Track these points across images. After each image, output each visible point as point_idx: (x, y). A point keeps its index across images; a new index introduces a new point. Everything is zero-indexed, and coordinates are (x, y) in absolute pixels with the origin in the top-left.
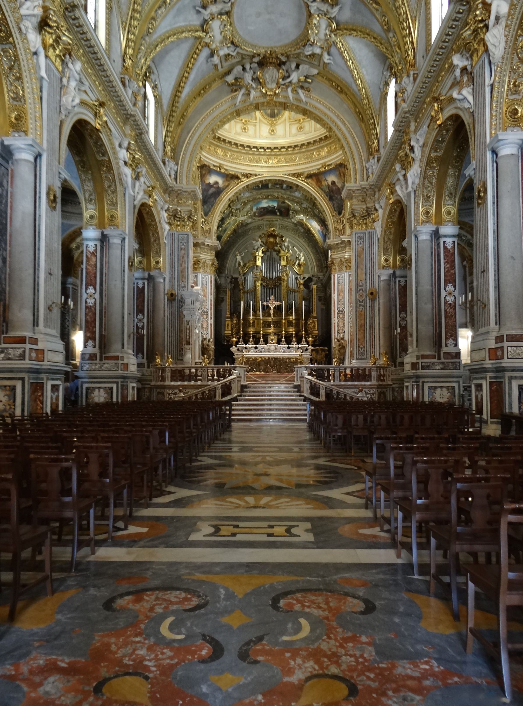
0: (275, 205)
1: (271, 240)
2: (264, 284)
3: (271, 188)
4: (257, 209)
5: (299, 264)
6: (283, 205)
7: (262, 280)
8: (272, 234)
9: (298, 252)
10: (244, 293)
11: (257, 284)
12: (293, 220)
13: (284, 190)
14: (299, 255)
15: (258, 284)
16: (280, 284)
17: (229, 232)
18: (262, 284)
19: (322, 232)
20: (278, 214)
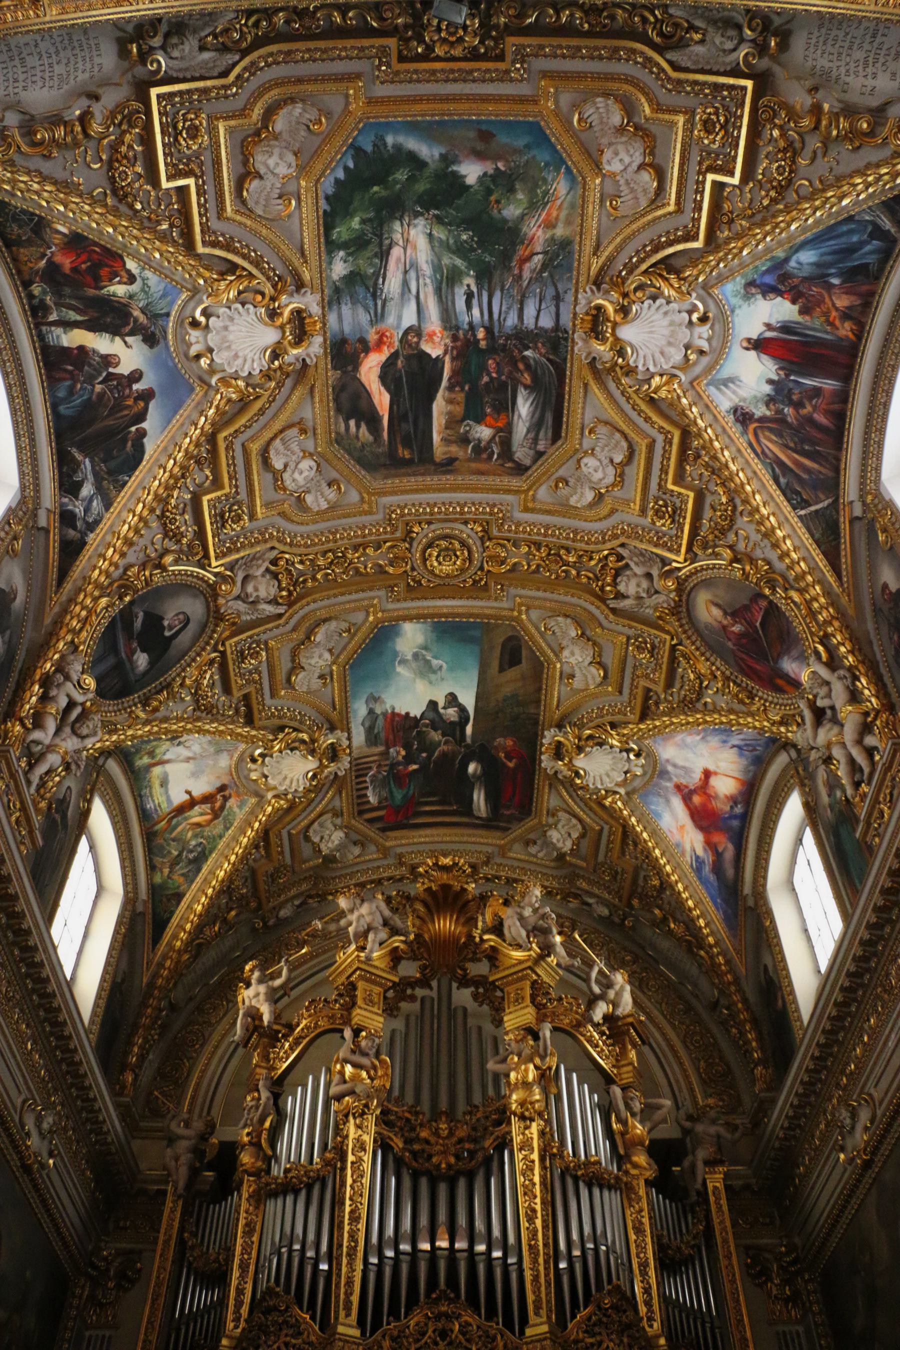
0: (468, 700)
1: (445, 925)
2: (398, 1143)
3: (448, 465)
4: (372, 738)
5: (607, 1018)
6: (510, 682)
7: (385, 1119)
8: (446, 888)
9: (600, 964)
10: (259, 1198)
11: (352, 1131)
12: (554, 835)
13: (520, 470)
14: (607, 984)
15: (361, 1134)
16: (504, 1143)
17: (219, 869)
18: (382, 1144)
19: (717, 868)
20: (479, 798)
